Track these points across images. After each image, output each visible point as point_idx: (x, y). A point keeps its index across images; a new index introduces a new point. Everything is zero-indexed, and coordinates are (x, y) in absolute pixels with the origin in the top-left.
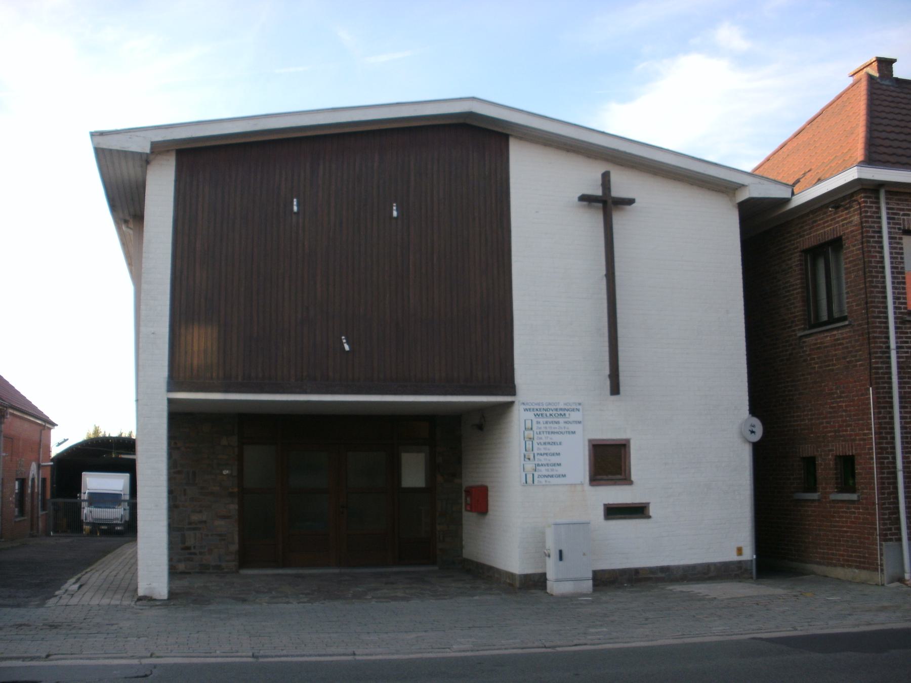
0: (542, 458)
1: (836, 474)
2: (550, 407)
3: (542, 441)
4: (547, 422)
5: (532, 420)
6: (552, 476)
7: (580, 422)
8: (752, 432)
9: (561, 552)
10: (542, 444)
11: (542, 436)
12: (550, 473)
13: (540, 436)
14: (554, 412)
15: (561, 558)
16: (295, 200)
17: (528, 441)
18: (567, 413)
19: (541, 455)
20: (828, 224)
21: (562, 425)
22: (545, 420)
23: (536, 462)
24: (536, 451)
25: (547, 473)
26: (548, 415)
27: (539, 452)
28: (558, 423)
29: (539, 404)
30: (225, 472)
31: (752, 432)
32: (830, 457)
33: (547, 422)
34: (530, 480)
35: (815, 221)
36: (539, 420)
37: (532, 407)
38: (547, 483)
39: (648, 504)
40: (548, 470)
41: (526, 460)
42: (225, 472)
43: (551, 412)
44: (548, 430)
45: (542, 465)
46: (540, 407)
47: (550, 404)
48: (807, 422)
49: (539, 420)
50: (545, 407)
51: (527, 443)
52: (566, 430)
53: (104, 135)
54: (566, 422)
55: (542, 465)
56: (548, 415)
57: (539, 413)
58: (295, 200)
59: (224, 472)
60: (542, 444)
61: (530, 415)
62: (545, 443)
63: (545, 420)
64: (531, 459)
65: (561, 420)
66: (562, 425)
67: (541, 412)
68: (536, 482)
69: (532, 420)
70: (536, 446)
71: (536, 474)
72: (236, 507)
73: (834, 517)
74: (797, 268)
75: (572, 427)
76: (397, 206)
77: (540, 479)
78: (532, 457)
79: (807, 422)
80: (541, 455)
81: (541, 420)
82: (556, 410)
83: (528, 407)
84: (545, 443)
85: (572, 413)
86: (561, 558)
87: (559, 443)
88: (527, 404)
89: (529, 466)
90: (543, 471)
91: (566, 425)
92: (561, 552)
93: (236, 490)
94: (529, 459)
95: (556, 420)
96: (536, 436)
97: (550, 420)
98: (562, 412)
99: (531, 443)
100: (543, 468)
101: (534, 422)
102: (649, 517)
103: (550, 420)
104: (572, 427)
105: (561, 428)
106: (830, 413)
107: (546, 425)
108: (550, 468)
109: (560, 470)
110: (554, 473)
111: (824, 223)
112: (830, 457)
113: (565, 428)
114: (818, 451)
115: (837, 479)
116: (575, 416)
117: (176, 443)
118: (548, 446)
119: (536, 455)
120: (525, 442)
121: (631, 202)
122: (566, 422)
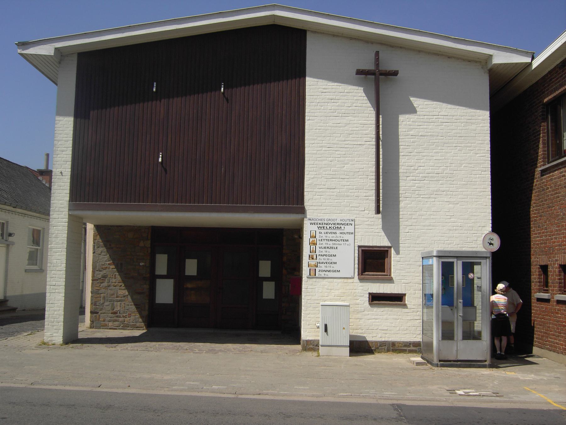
0: (322, 257)
1: (559, 279)
2: (329, 222)
3: (323, 246)
4: (327, 233)
5: (316, 231)
6: (329, 271)
7: (352, 233)
8: (491, 244)
9: (326, 326)
10: (323, 248)
11: (323, 242)
12: (328, 269)
13: (321, 242)
14: (333, 226)
15: (326, 330)
16: (155, 83)
17: (312, 245)
18: (342, 227)
19: (322, 255)
20: (559, 80)
21: (338, 235)
22: (326, 231)
23: (318, 261)
24: (317, 253)
25: (326, 269)
26: (328, 227)
27: (321, 254)
28: (336, 233)
29: (321, 220)
30: (141, 264)
31: (491, 244)
32: (556, 265)
33: (327, 233)
34: (312, 273)
35: (551, 80)
36: (321, 231)
37: (316, 222)
38: (326, 276)
39: (405, 295)
40: (326, 267)
41: (310, 259)
42: (141, 264)
43: (330, 226)
44: (328, 238)
45: (322, 263)
46: (322, 222)
47: (329, 220)
48: (544, 237)
49: (321, 231)
50: (326, 222)
51: (312, 247)
52: (341, 238)
53: (25, 45)
54: (341, 233)
55: (322, 263)
56: (328, 227)
57: (321, 226)
58: (155, 83)
59: (141, 264)
60: (323, 248)
61: (315, 227)
62: (325, 248)
63: (326, 231)
64: (314, 259)
65: (338, 232)
66: (338, 235)
67: (323, 226)
68: (317, 275)
69: (316, 231)
70: (318, 249)
71: (317, 269)
72: (148, 287)
73: (557, 313)
74: (540, 118)
75: (346, 237)
76: (224, 85)
77: (321, 273)
78: (315, 257)
79: (544, 237)
80: (322, 255)
81: (323, 231)
82: (335, 224)
83: (313, 222)
84: (325, 248)
85: (346, 227)
86: (326, 330)
87: (335, 248)
88: (313, 219)
89: (313, 262)
90: (323, 267)
91: (342, 235)
92: (326, 326)
93: (148, 275)
94: (313, 258)
95: (334, 231)
96: (318, 242)
97: (330, 231)
98: (338, 226)
99: (314, 247)
100: (323, 265)
101: (317, 233)
102: (405, 306)
103: (330, 231)
104: (346, 237)
105: (338, 237)
106: (557, 230)
107: (326, 235)
108: (328, 265)
109: (336, 267)
110: (332, 269)
111: (556, 80)
112: (556, 265)
113: (340, 237)
114: (549, 261)
115: (560, 283)
116: (350, 229)
117: (110, 245)
118: (328, 250)
119: (318, 256)
120: (310, 246)
121: (395, 73)
122: (341, 233)
